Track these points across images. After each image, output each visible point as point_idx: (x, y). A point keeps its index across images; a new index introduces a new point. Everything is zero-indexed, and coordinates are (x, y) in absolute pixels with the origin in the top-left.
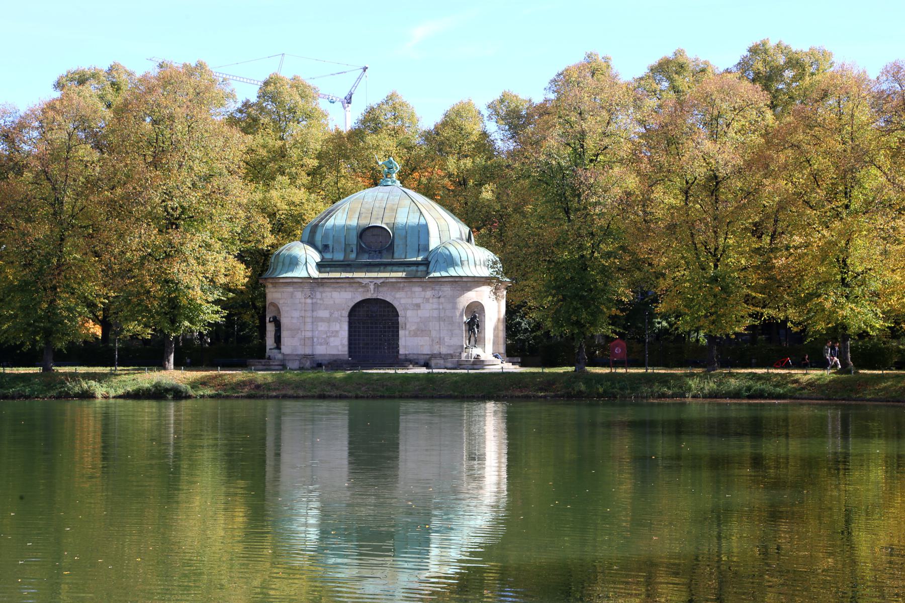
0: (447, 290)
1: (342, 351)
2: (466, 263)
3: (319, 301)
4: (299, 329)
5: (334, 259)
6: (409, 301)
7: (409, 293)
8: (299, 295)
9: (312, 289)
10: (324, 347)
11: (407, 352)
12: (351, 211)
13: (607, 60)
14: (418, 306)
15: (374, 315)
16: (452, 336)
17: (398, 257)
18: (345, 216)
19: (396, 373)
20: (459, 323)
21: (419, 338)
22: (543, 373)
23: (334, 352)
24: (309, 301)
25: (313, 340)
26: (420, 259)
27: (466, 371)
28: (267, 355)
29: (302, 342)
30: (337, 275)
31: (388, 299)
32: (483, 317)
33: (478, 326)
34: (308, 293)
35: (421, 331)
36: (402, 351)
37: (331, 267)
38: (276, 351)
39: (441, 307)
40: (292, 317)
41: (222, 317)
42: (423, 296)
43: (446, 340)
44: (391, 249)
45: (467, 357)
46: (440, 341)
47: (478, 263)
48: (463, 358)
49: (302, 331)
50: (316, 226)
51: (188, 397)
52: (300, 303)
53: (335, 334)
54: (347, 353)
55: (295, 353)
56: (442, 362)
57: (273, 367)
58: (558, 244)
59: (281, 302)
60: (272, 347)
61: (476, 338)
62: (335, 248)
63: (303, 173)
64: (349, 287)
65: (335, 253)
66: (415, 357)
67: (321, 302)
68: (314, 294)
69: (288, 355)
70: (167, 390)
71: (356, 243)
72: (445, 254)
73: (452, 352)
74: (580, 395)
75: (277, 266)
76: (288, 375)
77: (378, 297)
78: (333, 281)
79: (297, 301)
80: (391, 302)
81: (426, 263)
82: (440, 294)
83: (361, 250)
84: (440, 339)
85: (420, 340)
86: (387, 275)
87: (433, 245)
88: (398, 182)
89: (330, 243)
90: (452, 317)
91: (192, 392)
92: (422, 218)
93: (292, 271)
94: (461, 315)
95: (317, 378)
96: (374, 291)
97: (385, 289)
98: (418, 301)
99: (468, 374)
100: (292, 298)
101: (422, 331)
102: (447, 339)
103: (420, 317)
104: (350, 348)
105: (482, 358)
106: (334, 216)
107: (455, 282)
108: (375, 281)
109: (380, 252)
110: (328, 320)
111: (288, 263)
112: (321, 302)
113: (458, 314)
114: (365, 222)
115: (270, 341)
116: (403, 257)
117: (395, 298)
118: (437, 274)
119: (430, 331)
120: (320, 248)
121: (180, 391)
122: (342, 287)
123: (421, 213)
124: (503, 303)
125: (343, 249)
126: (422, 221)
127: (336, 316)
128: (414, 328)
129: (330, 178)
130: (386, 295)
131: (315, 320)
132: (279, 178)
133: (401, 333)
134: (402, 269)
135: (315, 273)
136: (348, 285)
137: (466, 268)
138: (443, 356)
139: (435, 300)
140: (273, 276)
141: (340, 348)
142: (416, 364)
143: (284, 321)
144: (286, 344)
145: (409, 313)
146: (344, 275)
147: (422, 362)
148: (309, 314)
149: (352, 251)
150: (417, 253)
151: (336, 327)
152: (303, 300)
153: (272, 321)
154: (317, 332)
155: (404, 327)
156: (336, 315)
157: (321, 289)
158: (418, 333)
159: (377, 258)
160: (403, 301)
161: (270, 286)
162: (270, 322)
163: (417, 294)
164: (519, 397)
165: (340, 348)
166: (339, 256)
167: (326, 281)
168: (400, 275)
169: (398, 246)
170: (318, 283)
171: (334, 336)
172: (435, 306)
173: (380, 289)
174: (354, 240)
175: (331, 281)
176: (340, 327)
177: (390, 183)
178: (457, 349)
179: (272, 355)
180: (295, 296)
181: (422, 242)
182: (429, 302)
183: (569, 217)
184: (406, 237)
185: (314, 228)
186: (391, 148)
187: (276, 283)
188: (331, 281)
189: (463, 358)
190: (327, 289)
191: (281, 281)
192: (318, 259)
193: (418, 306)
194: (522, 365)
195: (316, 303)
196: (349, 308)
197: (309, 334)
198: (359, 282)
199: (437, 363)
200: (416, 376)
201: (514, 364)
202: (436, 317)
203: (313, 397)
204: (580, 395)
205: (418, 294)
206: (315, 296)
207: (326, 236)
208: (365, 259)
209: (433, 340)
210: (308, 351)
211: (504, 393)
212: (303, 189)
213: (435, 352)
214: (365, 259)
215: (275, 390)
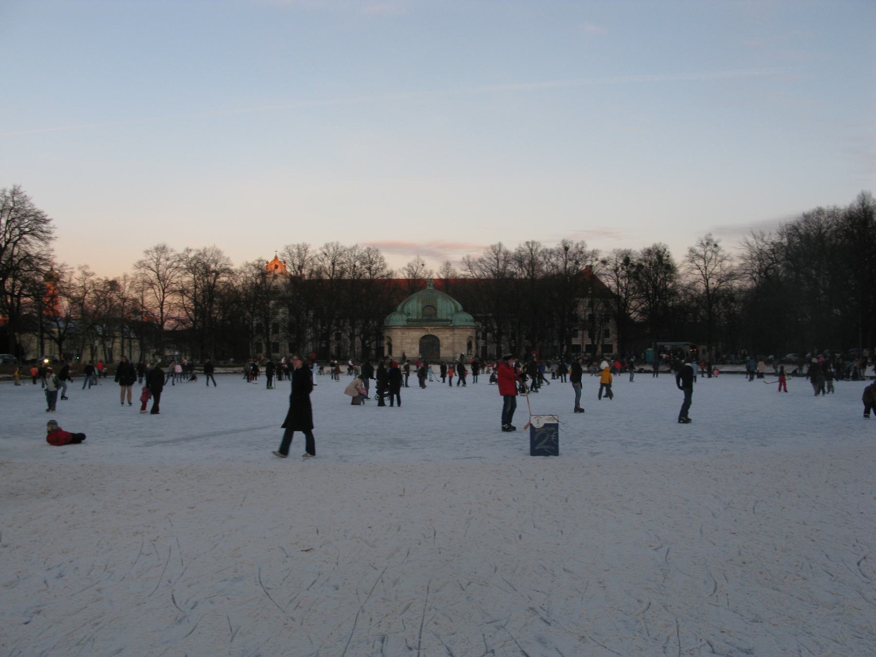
14: (447, 338)
17: (439, 316)
23: (414, 356)
24: (404, 335)
36: (441, 356)
53: (414, 349)
83: (424, 315)
89: (411, 312)
98: (448, 336)
130: (435, 334)
133: (441, 348)
143: (393, 343)
145: (445, 341)
151: (415, 346)
156: (414, 341)
160: (442, 336)
162: (387, 344)
166: (415, 317)
192: (406, 319)
205: (448, 333)
208: (425, 318)
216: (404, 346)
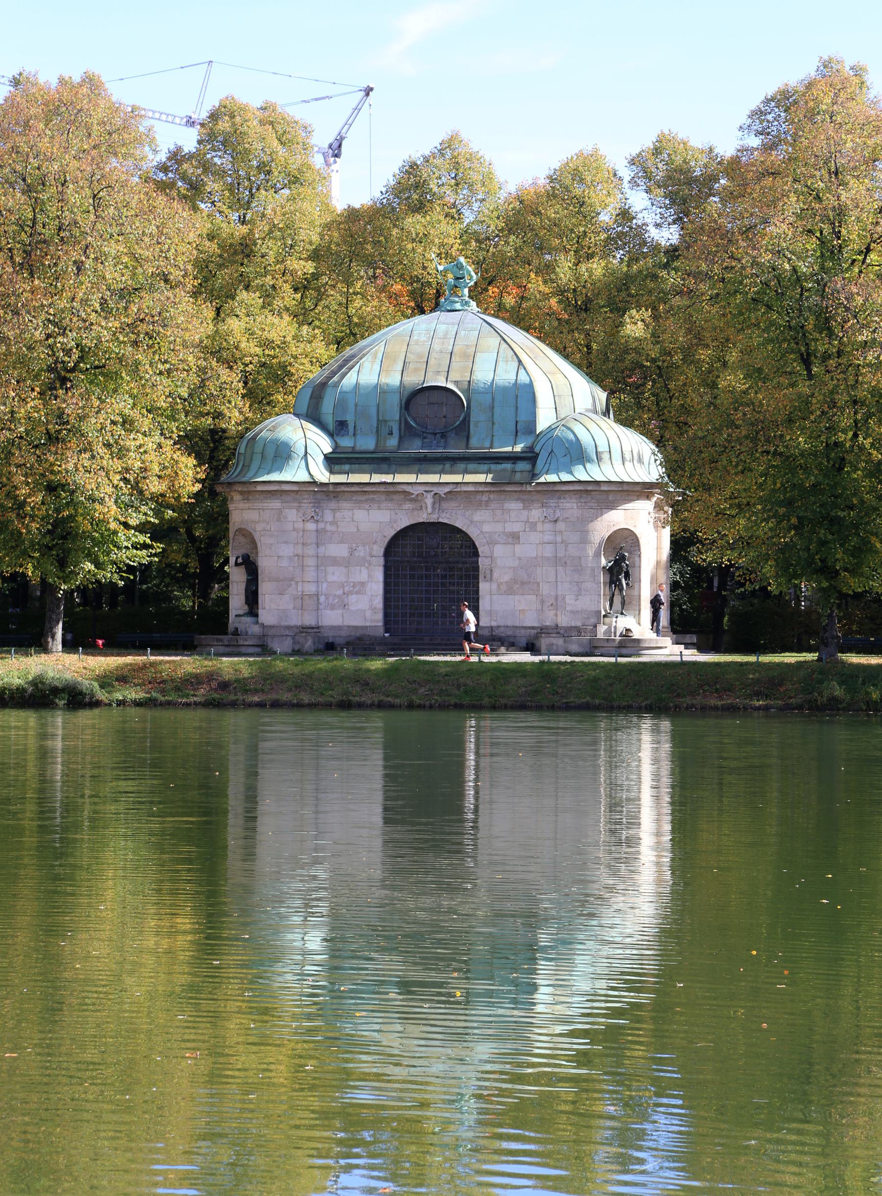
0: (571, 507)
1: (371, 621)
2: (606, 456)
3: (329, 527)
4: (292, 579)
5: (358, 448)
6: (499, 528)
7: (499, 512)
8: (292, 515)
9: (317, 504)
11: (494, 624)
13: (858, 71)
14: (515, 537)
16: (578, 594)
17: (478, 443)
19: (480, 661)
20: (593, 570)
21: (517, 597)
22: (758, 664)
24: (311, 526)
25: (318, 599)
26: (518, 448)
27: (613, 660)
28: (231, 626)
30: (364, 478)
32: (637, 559)
33: (627, 576)
34: (310, 512)
35: (513, 587)
37: (351, 464)
38: (249, 619)
39: (559, 539)
40: (279, 557)
41: (152, 555)
42: (525, 519)
43: (568, 601)
44: (463, 429)
45: (608, 632)
46: (557, 603)
47: (628, 456)
48: (600, 635)
50: (323, 385)
51: (95, 704)
52: (294, 530)
54: (381, 624)
55: (284, 623)
56: (560, 642)
57: (243, 650)
58: (790, 421)
59: (259, 527)
60: (241, 612)
61: (623, 598)
62: (358, 427)
63: (287, 287)
64: (386, 500)
65: (358, 437)
66: (510, 633)
67: (334, 528)
68: (320, 514)
70: (56, 691)
71: (397, 417)
72: (567, 440)
73: (579, 624)
74: (833, 706)
75: (251, 460)
76: (279, 665)
77: (441, 520)
80: (464, 529)
81: (530, 456)
82: (558, 514)
83: (407, 432)
84: (556, 599)
85: (520, 601)
86: (457, 478)
87: (542, 425)
88: (473, 304)
89: (350, 418)
90: (580, 558)
91: (101, 695)
92: (522, 371)
93: (280, 469)
94: (597, 555)
95: (334, 670)
96: (433, 508)
97: (453, 504)
98: (516, 527)
99: (616, 664)
100: (279, 520)
102: (570, 600)
103: (520, 558)
104: (386, 615)
105: (636, 635)
106: (356, 368)
107: (587, 491)
108: (436, 490)
109: (443, 436)
110: (346, 563)
111: (272, 455)
112: (334, 528)
113: (591, 552)
114: (414, 379)
115: (237, 602)
116: (487, 444)
118: (552, 478)
119: (538, 584)
120: (331, 426)
121: (81, 693)
123: (520, 362)
124: (666, 533)
126: (523, 378)
127: (362, 554)
128: (506, 578)
129: (334, 297)
131: (323, 562)
132: (243, 295)
134: (485, 467)
135: (322, 475)
136: (383, 497)
137: (606, 466)
138: (562, 631)
139: (548, 526)
140: (244, 479)
141: (368, 614)
142: (512, 645)
143: (265, 563)
146: (377, 478)
147: (523, 642)
148: (311, 551)
149: (391, 433)
150: (512, 438)
151: (362, 575)
152: (300, 525)
153: (241, 564)
154: (325, 585)
155: (488, 576)
156: (361, 552)
157: (333, 504)
158: (516, 586)
159: (438, 447)
160: (486, 528)
161: (237, 497)
162: (237, 564)
163: (513, 514)
164: (716, 708)
165: (368, 614)
166: (367, 443)
167: (343, 488)
168: (481, 478)
169: (477, 423)
170: (327, 494)
171: (357, 593)
172: (547, 538)
173: (445, 505)
174: (394, 413)
175: (353, 489)
176: (369, 576)
177: (458, 306)
179: (241, 628)
180: (285, 518)
181: (523, 417)
182: (536, 531)
183: (809, 370)
184: (492, 408)
185: (319, 390)
186: (451, 241)
187: (249, 492)
188: (353, 489)
189: (600, 635)
190: (345, 505)
191: (259, 488)
192: (328, 449)
193: (515, 537)
194: (702, 649)
195: (325, 531)
196: (387, 540)
197: (311, 589)
198: (405, 492)
199: (552, 644)
200: (519, 668)
201: (687, 646)
202: (548, 558)
203: (328, 706)
204: (833, 706)
207: (341, 404)
209: (543, 602)
210: (309, 620)
211: (688, 700)
212: (287, 318)
213: (548, 624)
214: (415, 448)
215: (256, 691)
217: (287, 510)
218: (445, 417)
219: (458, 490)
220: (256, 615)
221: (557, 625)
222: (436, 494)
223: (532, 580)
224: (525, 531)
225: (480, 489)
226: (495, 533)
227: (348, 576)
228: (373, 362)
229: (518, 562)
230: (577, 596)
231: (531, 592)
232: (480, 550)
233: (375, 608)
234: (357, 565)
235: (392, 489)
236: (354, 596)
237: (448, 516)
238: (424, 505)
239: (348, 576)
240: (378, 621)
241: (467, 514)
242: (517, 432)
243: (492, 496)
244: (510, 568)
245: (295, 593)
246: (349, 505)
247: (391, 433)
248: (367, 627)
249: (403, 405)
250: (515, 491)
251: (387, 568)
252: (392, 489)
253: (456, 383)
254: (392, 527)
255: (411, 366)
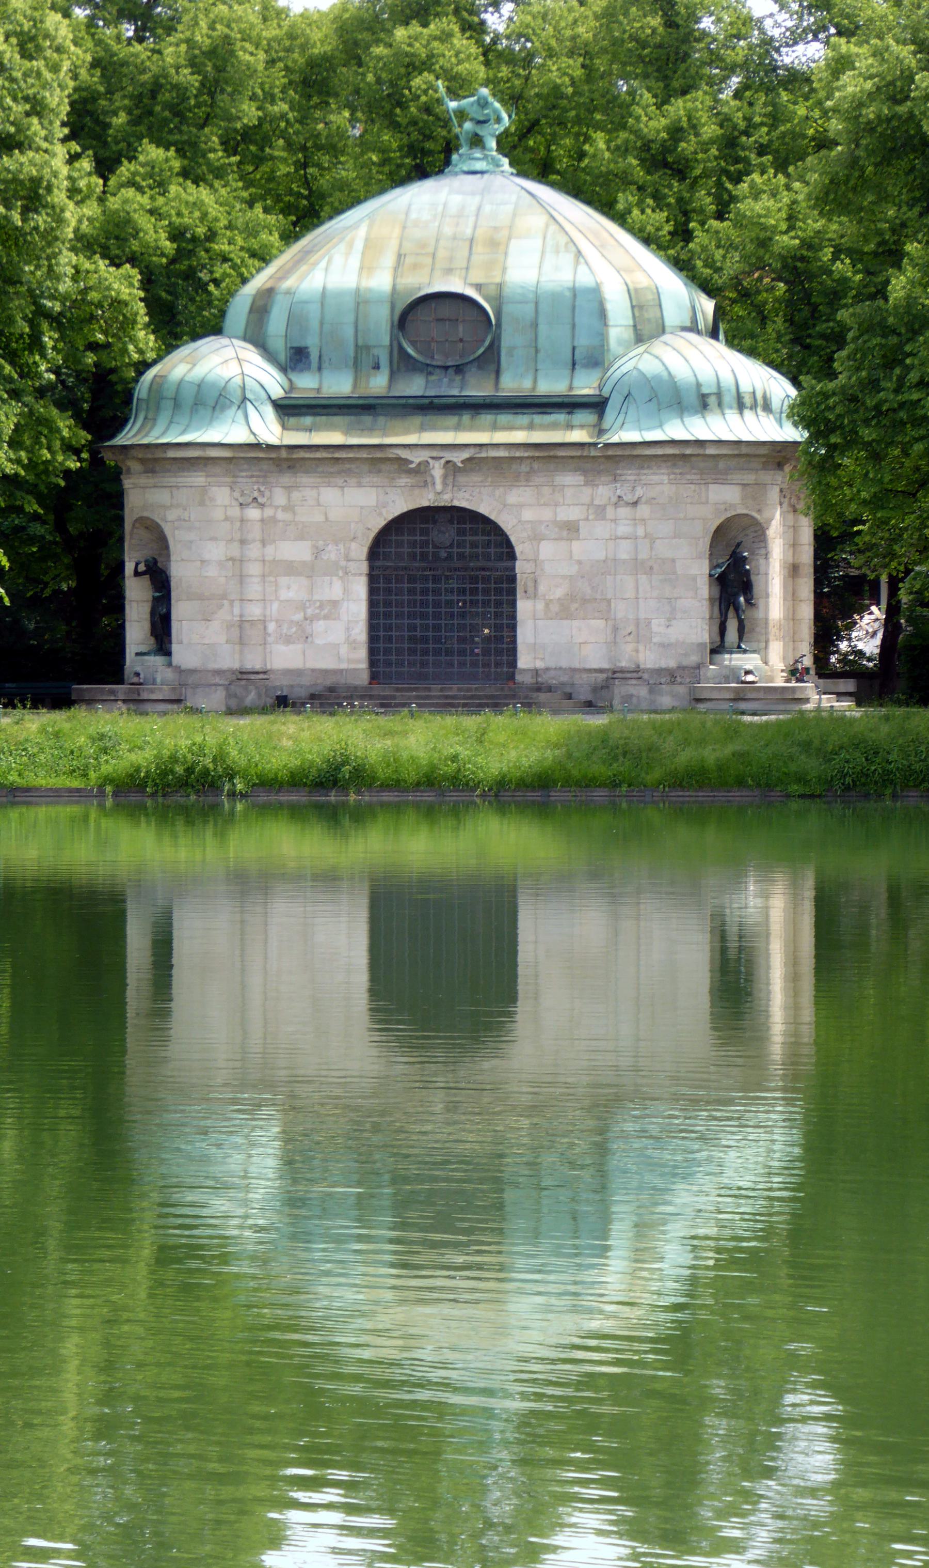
1: (349, 661)
2: (712, 401)
3: (280, 515)
4: (224, 596)
6: (546, 514)
7: (546, 490)
10: (299, 647)
11: (539, 664)
12: (371, 247)
14: (571, 529)
15: (443, 554)
18: (355, 261)
21: (575, 623)
24: (253, 513)
25: (265, 628)
29: (235, 632)
30: (336, 438)
31: (483, 509)
32: (762, 561)
36: (524, 661)
37: (314, 415)
38: (159, 660)
39: (640, 532)
40: (203, 562)
43: (655, 628)
49: (232, 602)
52: (227, 519)
53: (330, 609)
54: (364, 665)
59: (172, 515)
60: (143, 648)
62: (325, 358)
64: (370, 472)
66: (564, 679)
68: (267, 493)
69: (193, 671)
71: (386, 341)
77: (456, 503)
78: (670, 451)
79: (218, 514)
80: (493, 517)
82: (639, 492)
84: (637, 625)
86: (482, 437)
89: (312, 342)
90: (673, 561)
96: (445, 484)
97: (476, 478)
101: (585, 601)
102: (657, 626)
103: (579, 562)
104: (372, 652)
106: (323, 264)
107: (684, 456)
117: (505, 506)
119: (609, 601)
120: (282, 357)
122: (349, 472)
125: (351, 363)
126: (585, 279)
127: (333, 557)
128: (559, 593)
136: (366, 467)
138: (646, 676)
139: (624, 512)
144: (185, 641)
145: (547, 550)
147: (584, 694)
150: (569, 372)
151: (333, 589)
154: (275, 606)
155: (531, 590)
157: (286, 479)
160: (528, 515)
162: (137, 573)
165: (344, 650)
167: (302, 454)
169: (511, 349)
171: (326, 617)
172: (623, 529)
173: (462, 479)
175: (318, 455)
178: (686, 655)
180: (212, 499)
181: (583, 341)
184: (535, 325)
187: (156, 460)
188: (318, 455)
190: (304, 479)
193: (571, 529)
196: (372, 535)
198: (399, 459)
202: (624, 561)
206: (270, 498)
209: (615, 629)
210: (253, 662)
216: (254, 589)
217: (214, 489)
218: (461, 340)
219: (483, 455)
220: (168, 654)
221: (638, 666)
222: (448, 462)
223: (598, 597)
224: (587, 519)
225: (518, 454)
226: (541, 522)
227: (311, 591)
228: (348, 254)
229: (576, 567)
230: (669, 620)
231: (597, 614)
232: (518, 550)
233: (354, 641)
234: (325, 575)
235: (379, 455)
236: (321, 622)
237: (467, 496)
238: (429, 480)
239: (311, 591)
240: (358, 661)
241: (497, 493)
242: (574, 364)
243: (536, 465)
244: (564, 577)
245: (229, 618)
246: (312, 480)
247: (377, 367)
248: (341, 671)
249: (396, 322)
250: (572, 457)
251: (372, 579)
252: (379, 455)
253: (478, 287)
254: (380, 514)
255: (409, 260)
